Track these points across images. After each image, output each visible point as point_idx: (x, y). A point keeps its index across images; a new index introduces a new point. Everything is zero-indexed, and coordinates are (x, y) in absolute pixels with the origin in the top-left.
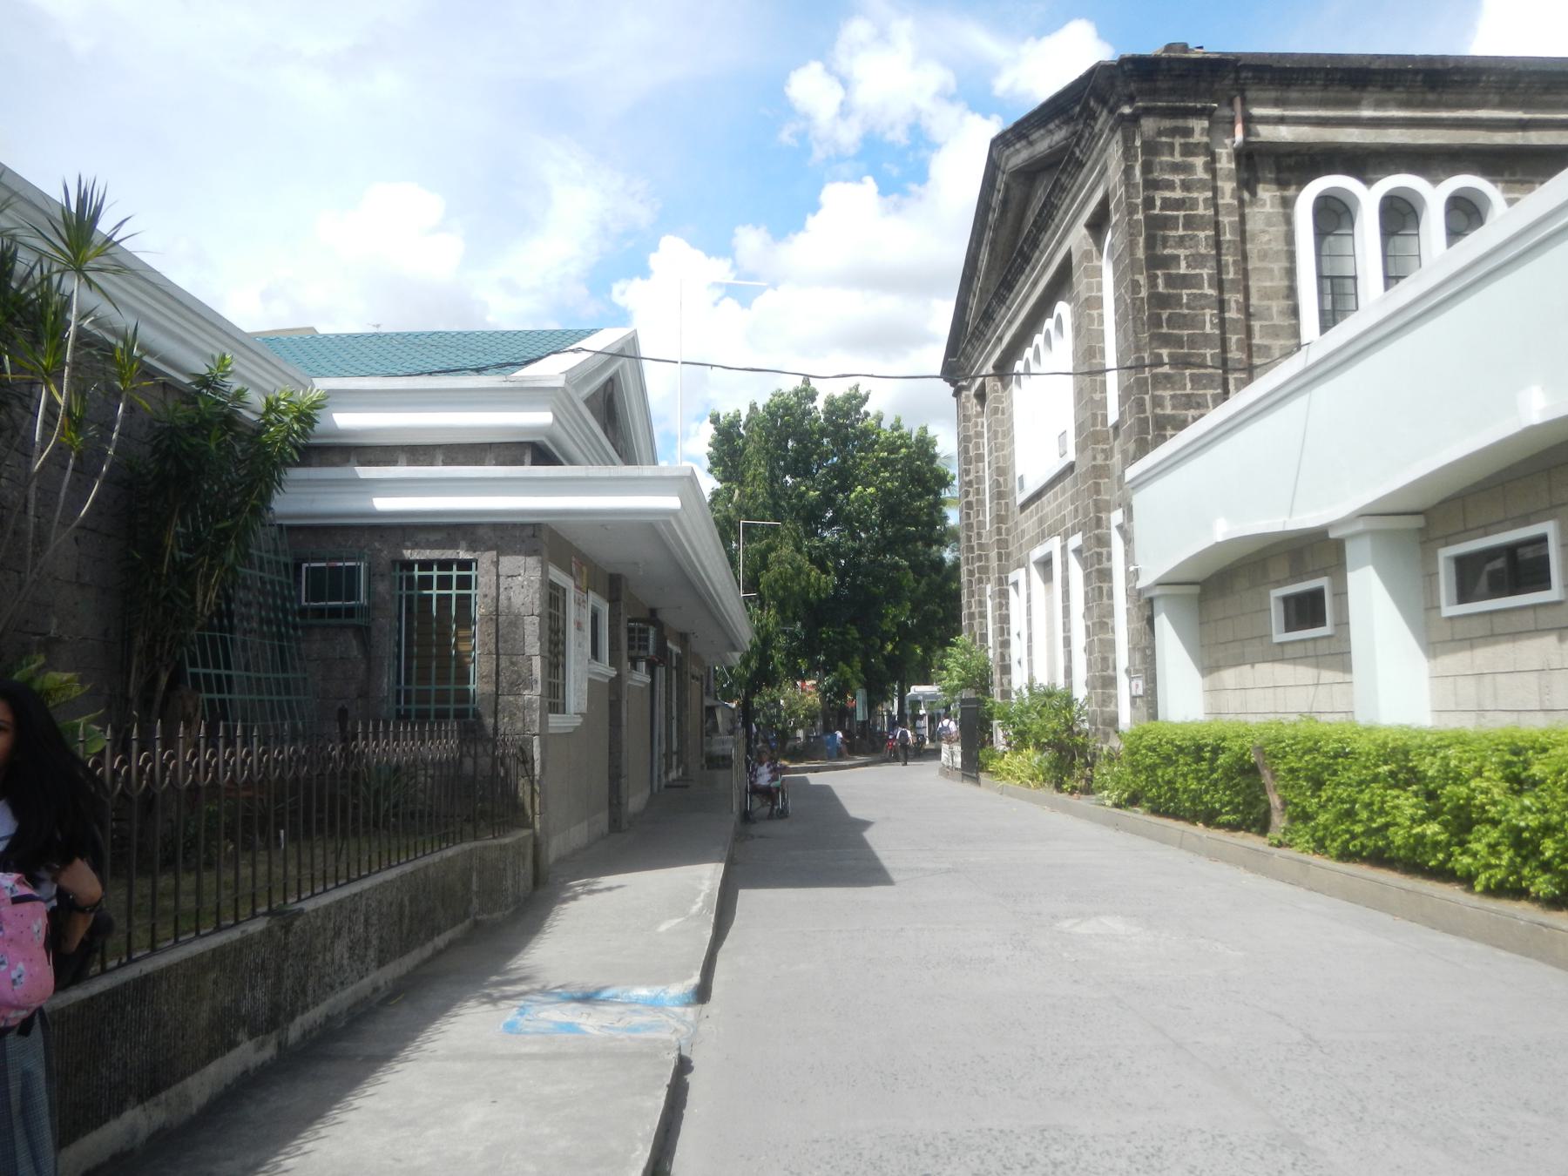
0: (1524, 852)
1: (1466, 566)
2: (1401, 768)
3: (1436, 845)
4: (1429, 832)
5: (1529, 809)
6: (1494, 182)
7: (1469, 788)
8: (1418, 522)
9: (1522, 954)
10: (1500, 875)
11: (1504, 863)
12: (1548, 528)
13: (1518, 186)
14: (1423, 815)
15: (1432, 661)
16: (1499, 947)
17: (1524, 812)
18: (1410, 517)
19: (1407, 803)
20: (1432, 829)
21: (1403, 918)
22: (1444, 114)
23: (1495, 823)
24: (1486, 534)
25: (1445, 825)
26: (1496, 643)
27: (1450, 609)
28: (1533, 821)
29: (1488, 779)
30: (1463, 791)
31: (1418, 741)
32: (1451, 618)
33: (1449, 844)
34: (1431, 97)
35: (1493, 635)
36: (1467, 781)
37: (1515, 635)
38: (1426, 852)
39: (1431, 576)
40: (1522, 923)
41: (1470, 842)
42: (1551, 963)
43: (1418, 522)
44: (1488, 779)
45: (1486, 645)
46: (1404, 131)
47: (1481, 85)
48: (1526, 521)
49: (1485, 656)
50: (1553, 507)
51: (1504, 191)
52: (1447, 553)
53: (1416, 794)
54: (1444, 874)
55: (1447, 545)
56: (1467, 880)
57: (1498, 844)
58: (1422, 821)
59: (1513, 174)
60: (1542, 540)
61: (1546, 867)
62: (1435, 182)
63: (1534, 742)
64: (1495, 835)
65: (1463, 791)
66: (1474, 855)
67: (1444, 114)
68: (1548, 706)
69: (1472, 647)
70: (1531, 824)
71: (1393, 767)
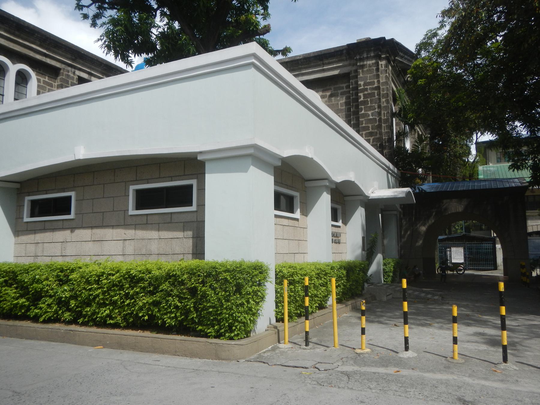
0: (61, 306)
1: (34, 203)
2: (10, 279)
3: (22, 306)
4: (20, 302)
5: (66, 290)
6: (33, 70)
7: (42, 285)
8: (18, 186)
9: (61, 342)
10: (50, 315)
11: (53, 310)
12: (73, 194)
13: (41, 75)
14: (18, 296)
15: (17, 238)
16: (51, 341)
17: (64, 292)
18: (16, 184)
19: (11, 292)
20: (22, 301)
21: (7, 336)
22: (21, 41)
23: (51, 296)
24: (46, 194)
25: (28, 299)
26: (46, 232)
27: (26, 219)
28: (67, 294)
29: (50, 281)
30: (40, 286)
31: (19, 269)
32: (27, 222)
33: (29, 306)
34: (17, 33)
35: (44, 229)
36: (42, 282)
37: (54, 230)
38: (17, 310)
39: (20, 207)
40: (62, 331)
41: (39, 304)
42: (73, 343)
43: (18, 186)
44: (50, 281)
45: (41, 233)
46: (5, 41)
47: (35, 36)
48: (63, 190)
49: (39, 237)
50: (74, 187)
51: (36, 75)
52: (28, 199)
53: (16, 288)
54: (24, 317)
55: (29, 195)
56: (35, 319)
57: (52, 304)
58: (17, 299)
59: (40, 70)
60: (70, 198)
61: (69, 310)
62: (14, 63)
63: (70, 267)
64: (50, 301)
65: (40, 286)
66: (41, 308)
67: (21, 41)
68: (64, 254)
69: (35, 233)
70: (67, 296)
71: (7, 278)
